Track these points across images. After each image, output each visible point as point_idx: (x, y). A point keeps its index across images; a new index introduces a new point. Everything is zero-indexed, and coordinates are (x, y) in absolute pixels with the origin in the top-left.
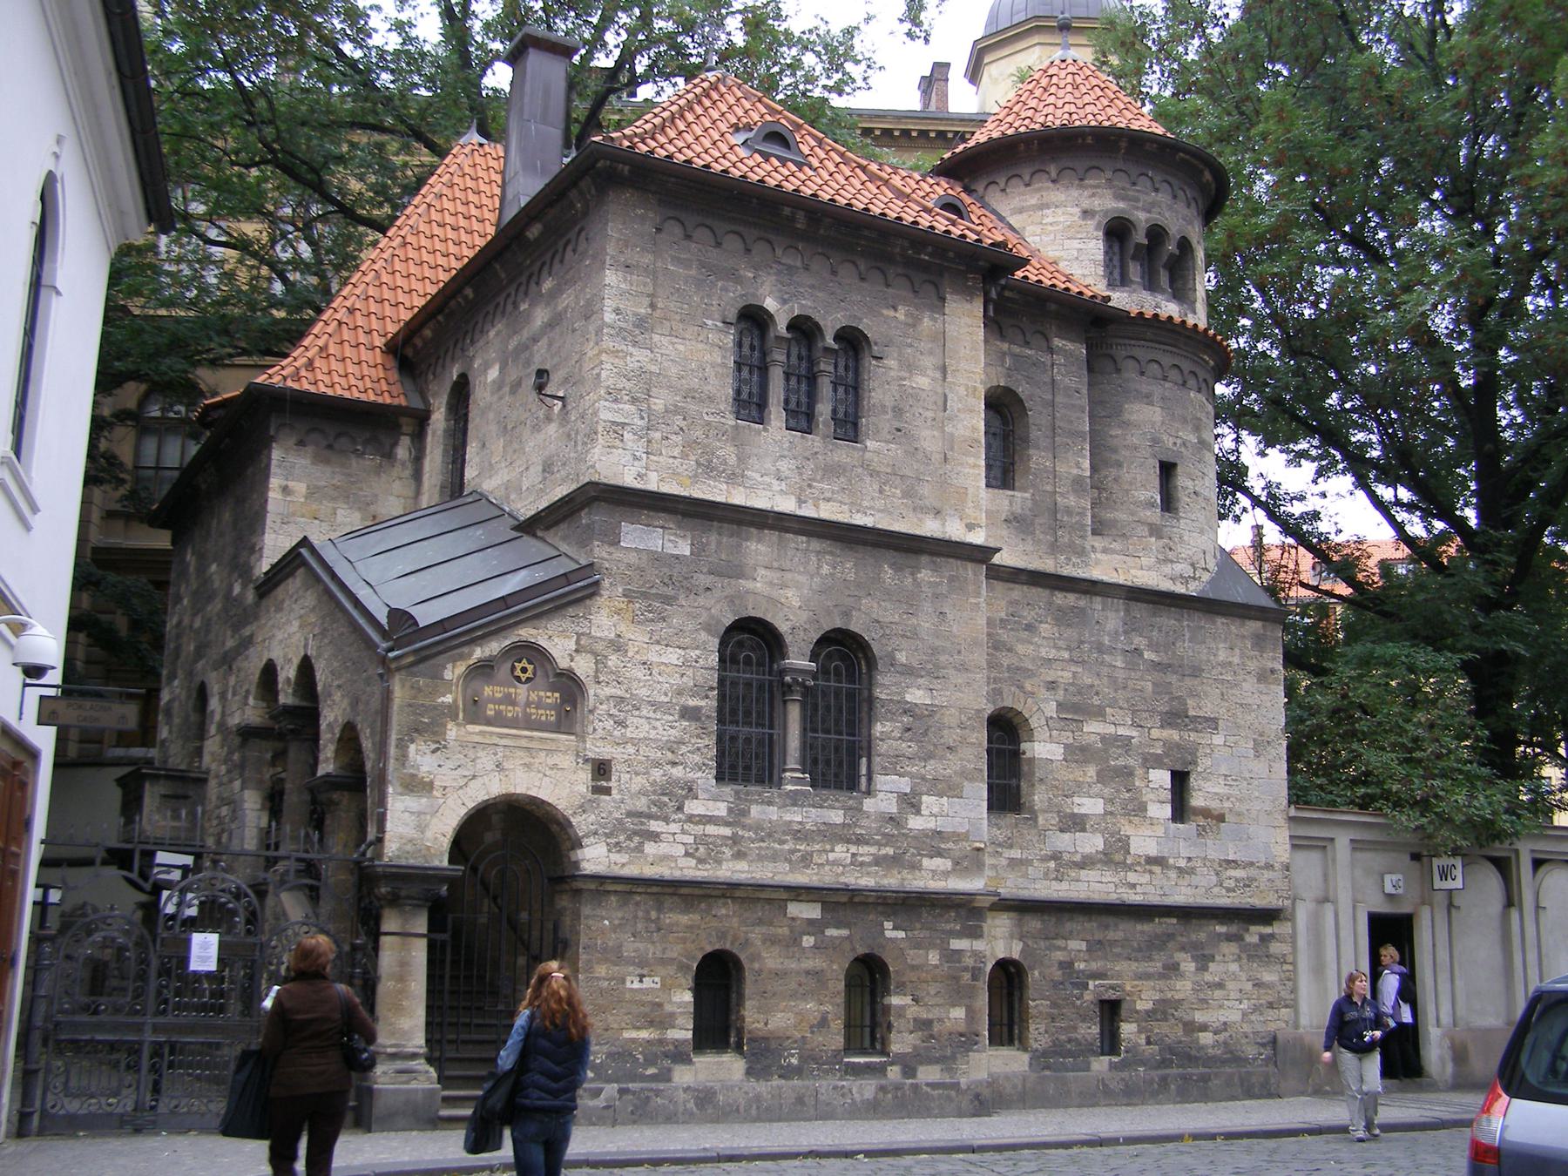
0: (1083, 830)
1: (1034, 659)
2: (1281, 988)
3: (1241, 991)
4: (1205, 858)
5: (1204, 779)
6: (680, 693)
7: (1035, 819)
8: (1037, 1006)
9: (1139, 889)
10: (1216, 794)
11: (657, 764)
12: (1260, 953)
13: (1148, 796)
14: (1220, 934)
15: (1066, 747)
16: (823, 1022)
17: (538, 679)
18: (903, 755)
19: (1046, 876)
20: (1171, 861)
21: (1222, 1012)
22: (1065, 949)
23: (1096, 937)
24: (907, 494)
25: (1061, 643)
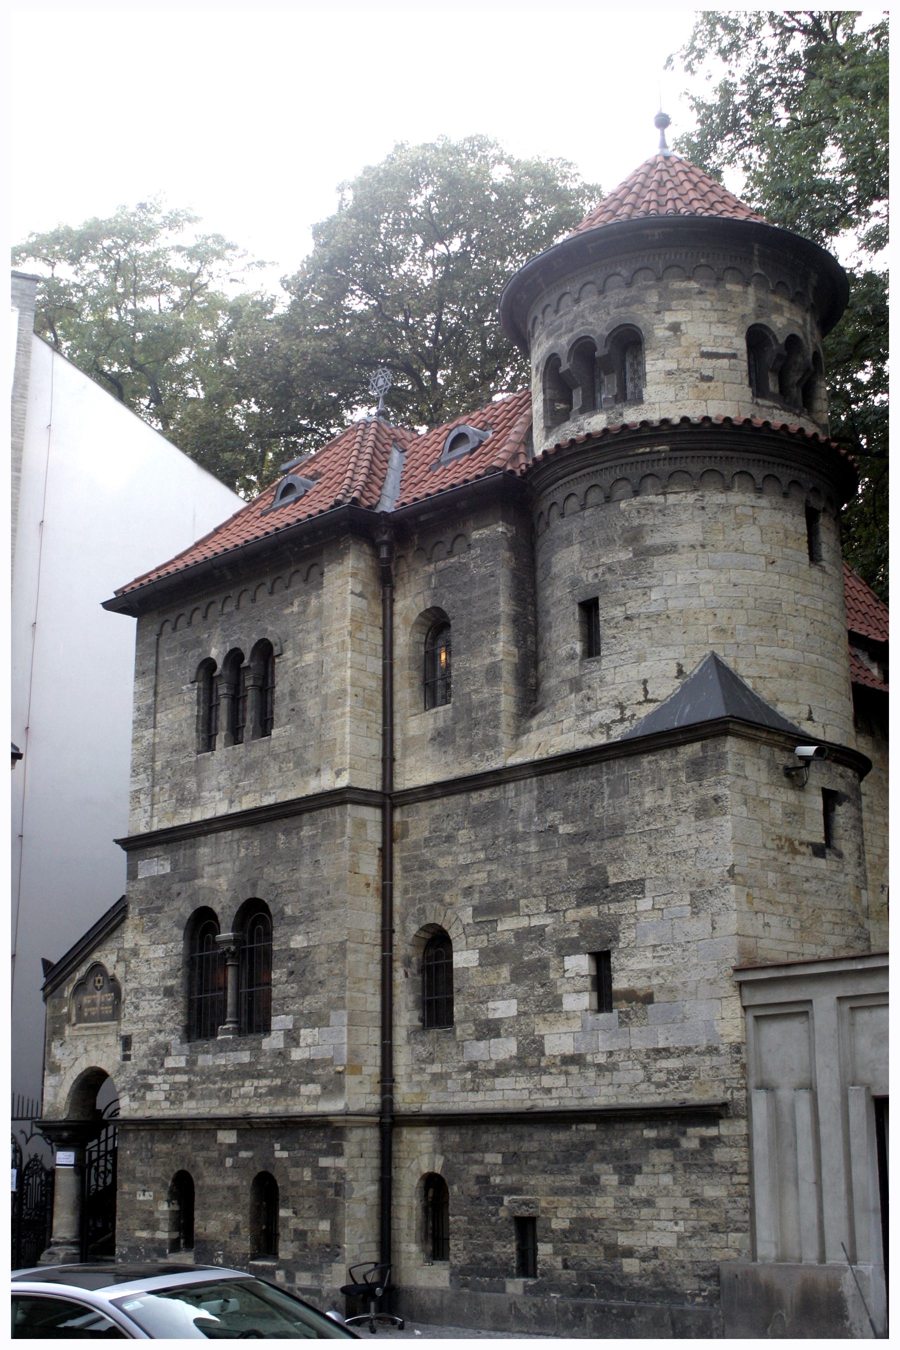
0: (498, 1036)
1: (452, 870)
2: (730, 1206)
3: (675, 1209)
4: (629, 1050)
5: (627, 955)
6: (164, 978)
7: (454, 1033)
8: (455, 1222)
9: (554, 1094)
10: (644, 970)
11: (151, 1033)
12: (700, 1162)
13: (563, 988)
14: (648, 1140)
15: (483, 952)
16: (236, 1231)
17: (105, 986)
18: (288, 997)
19: (463, 1089)
20: (589, 1058)
21: (651, 1234)
22: (482, 1162)
23: (512, 1149)
24: (297, 765)
25: (477, 845)
